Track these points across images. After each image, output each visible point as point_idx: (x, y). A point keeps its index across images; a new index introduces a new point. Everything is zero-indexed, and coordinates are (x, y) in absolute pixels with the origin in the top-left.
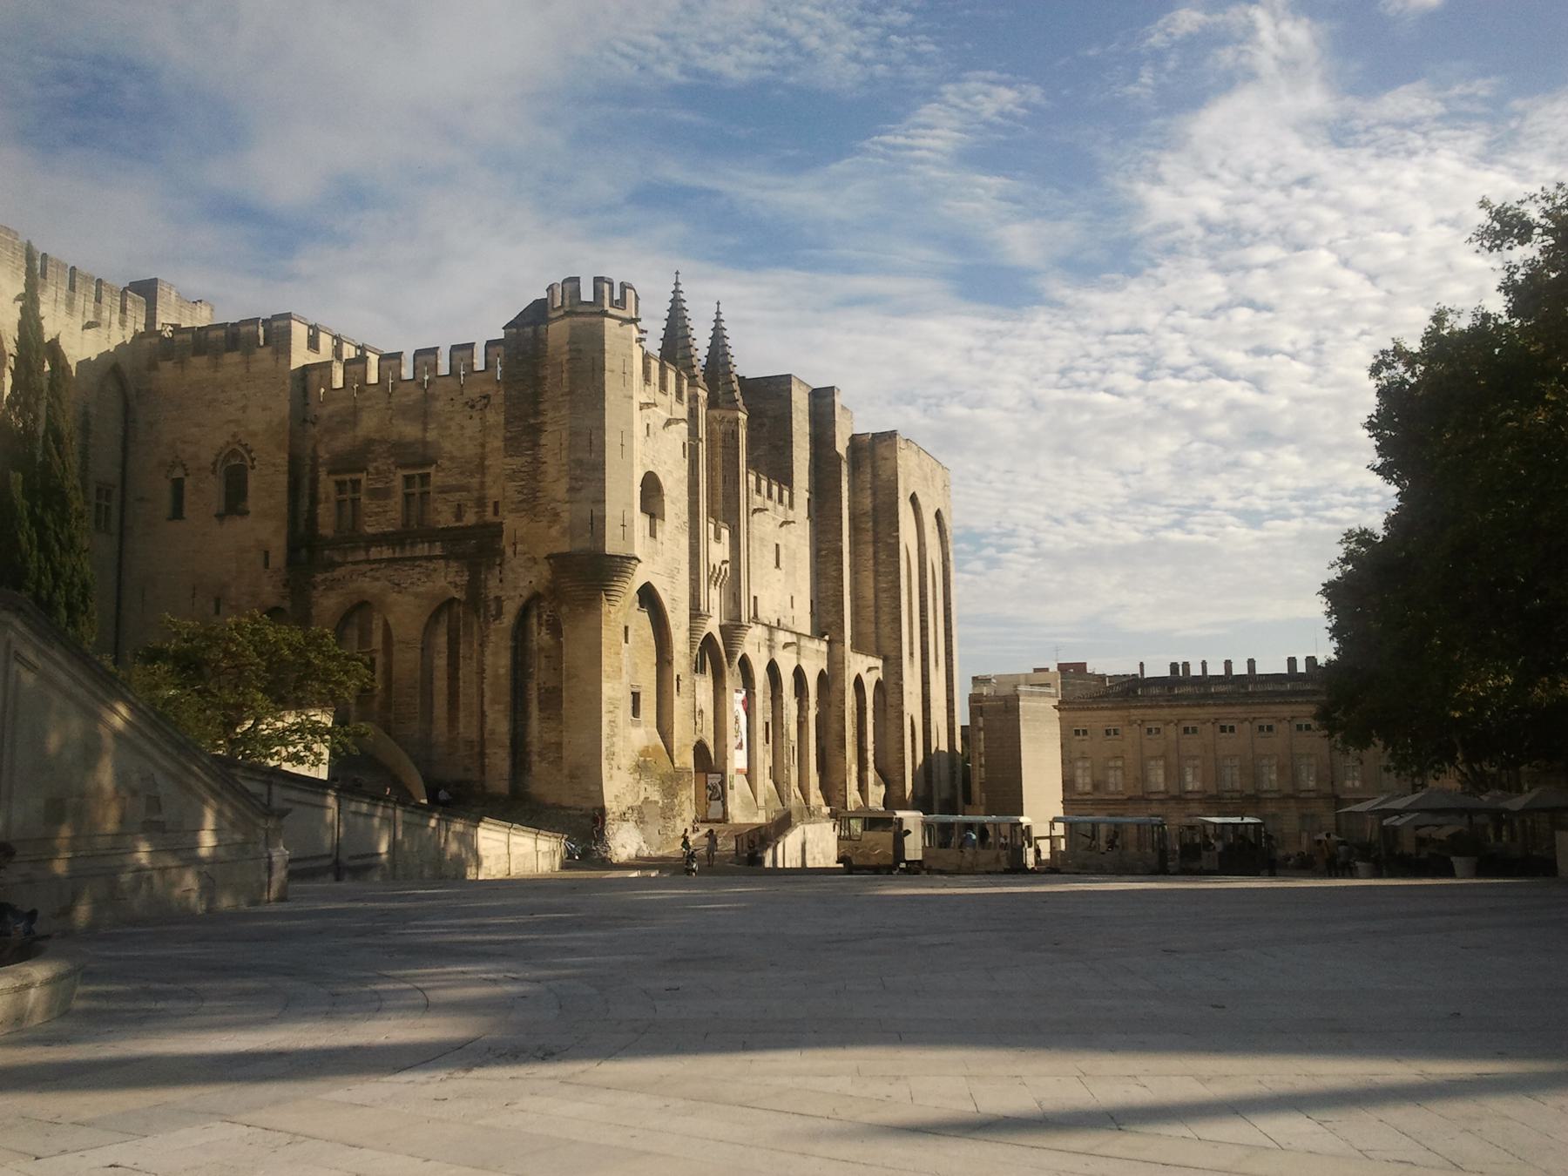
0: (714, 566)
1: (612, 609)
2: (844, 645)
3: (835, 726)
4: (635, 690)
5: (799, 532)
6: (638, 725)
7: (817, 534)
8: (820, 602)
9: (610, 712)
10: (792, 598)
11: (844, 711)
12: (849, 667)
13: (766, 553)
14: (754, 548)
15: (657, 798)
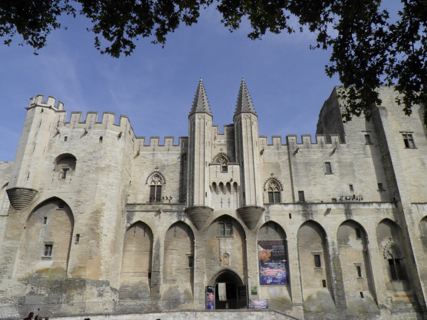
0: (221, 184)
1: (19, 212)
2: (401, 202)
3: (409, 250)
4: (49, 244)
5: (355, 152)
6: (50, 258)
7: (380, 150)
8: (389, 183)
9: (8, 253)
10: (351, 186)
11: (410, 240)
12: (410, 212)
13: (312, 169)
14: (296, 169)
15: (43, 293)
